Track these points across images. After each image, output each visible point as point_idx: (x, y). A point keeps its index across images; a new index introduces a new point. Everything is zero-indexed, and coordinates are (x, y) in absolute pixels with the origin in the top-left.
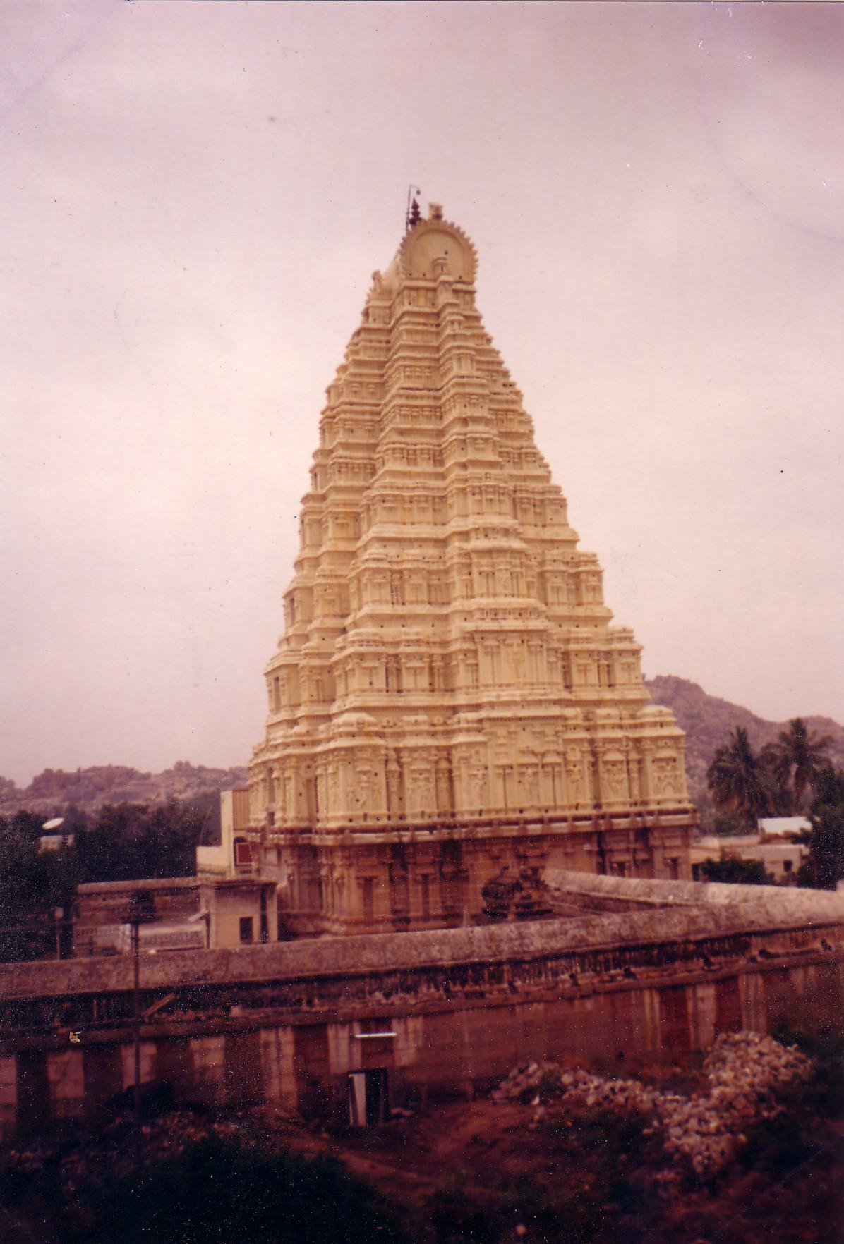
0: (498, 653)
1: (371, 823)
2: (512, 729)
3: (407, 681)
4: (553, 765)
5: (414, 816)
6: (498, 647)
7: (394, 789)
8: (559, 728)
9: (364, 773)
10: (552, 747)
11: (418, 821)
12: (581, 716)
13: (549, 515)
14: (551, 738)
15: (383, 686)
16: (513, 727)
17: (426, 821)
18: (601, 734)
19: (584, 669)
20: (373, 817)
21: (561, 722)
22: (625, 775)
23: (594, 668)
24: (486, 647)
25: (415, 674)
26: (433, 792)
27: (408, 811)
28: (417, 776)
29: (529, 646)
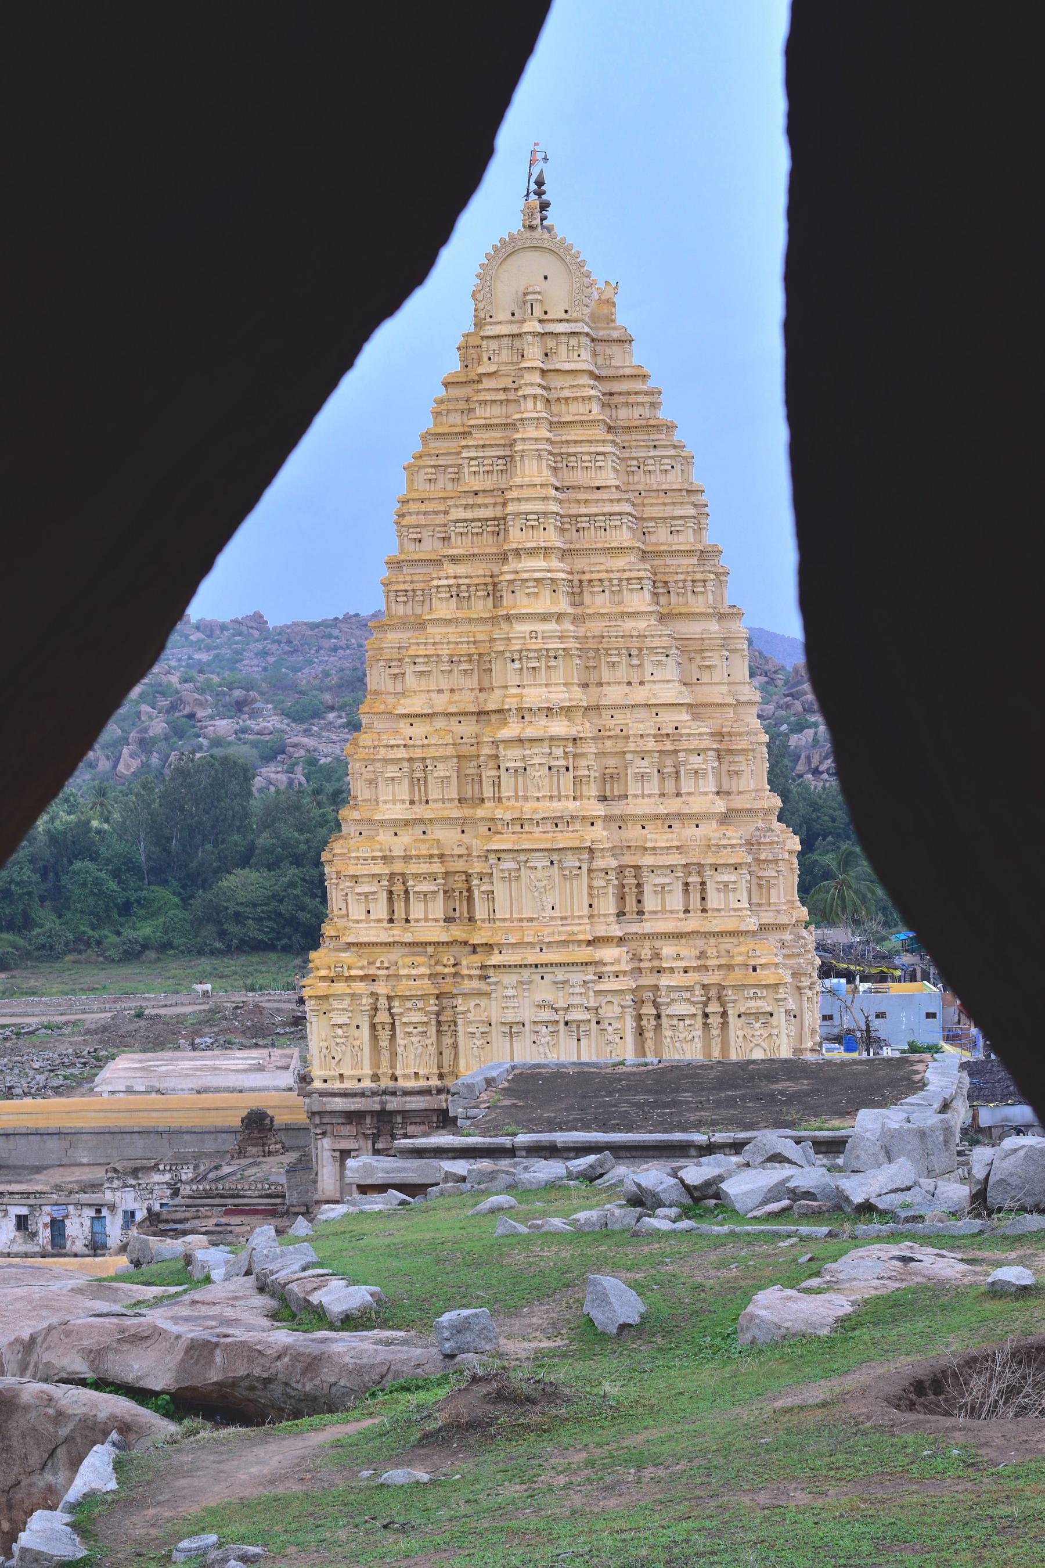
0: (518, 878)
1: (348, 1085)
2: (525, 978)
3: (417, 910)
4: (579, 1023)
5: (406, 1077)
6: (519, 869)
7: (384, 1043)
8: (591, 977)
9: (340, 1026)
10: (577, 1000)
11: (412, 1084)
12: (625, 958)
13: (648, 668)
14: (577, 990)
15: (385, 916)
16: (526, 973)
17: (422, 1083)
18: (665, 981)
19: (662, 890)
20: (351, 1077)
21: (591, 969)
22: (699, 1033)
23: (679, 887)
24: (502, 870)
25: (425, 901)
26: (432, 1050)
27: (398, 1072)
28: (411, 1029)
29: (562, 869)
